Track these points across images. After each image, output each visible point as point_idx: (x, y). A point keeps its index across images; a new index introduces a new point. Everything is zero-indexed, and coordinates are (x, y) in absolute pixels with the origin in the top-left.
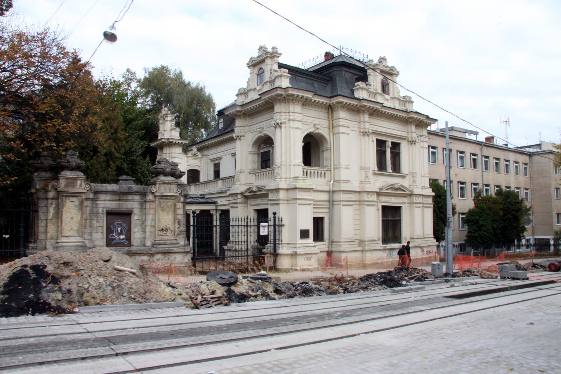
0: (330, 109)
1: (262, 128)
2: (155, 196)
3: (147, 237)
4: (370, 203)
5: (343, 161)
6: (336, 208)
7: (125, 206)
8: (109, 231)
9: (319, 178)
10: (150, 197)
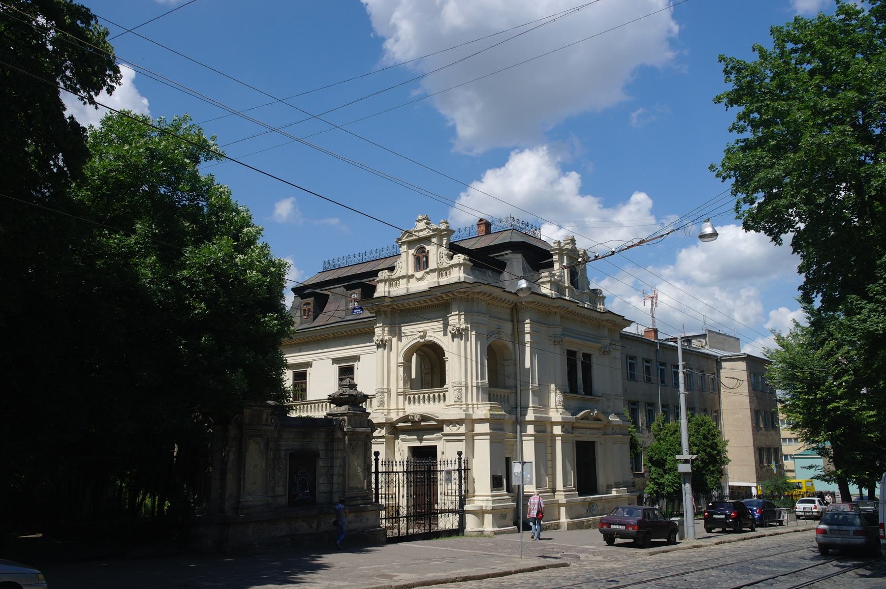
1: (425, 332)
3: (334, 490)
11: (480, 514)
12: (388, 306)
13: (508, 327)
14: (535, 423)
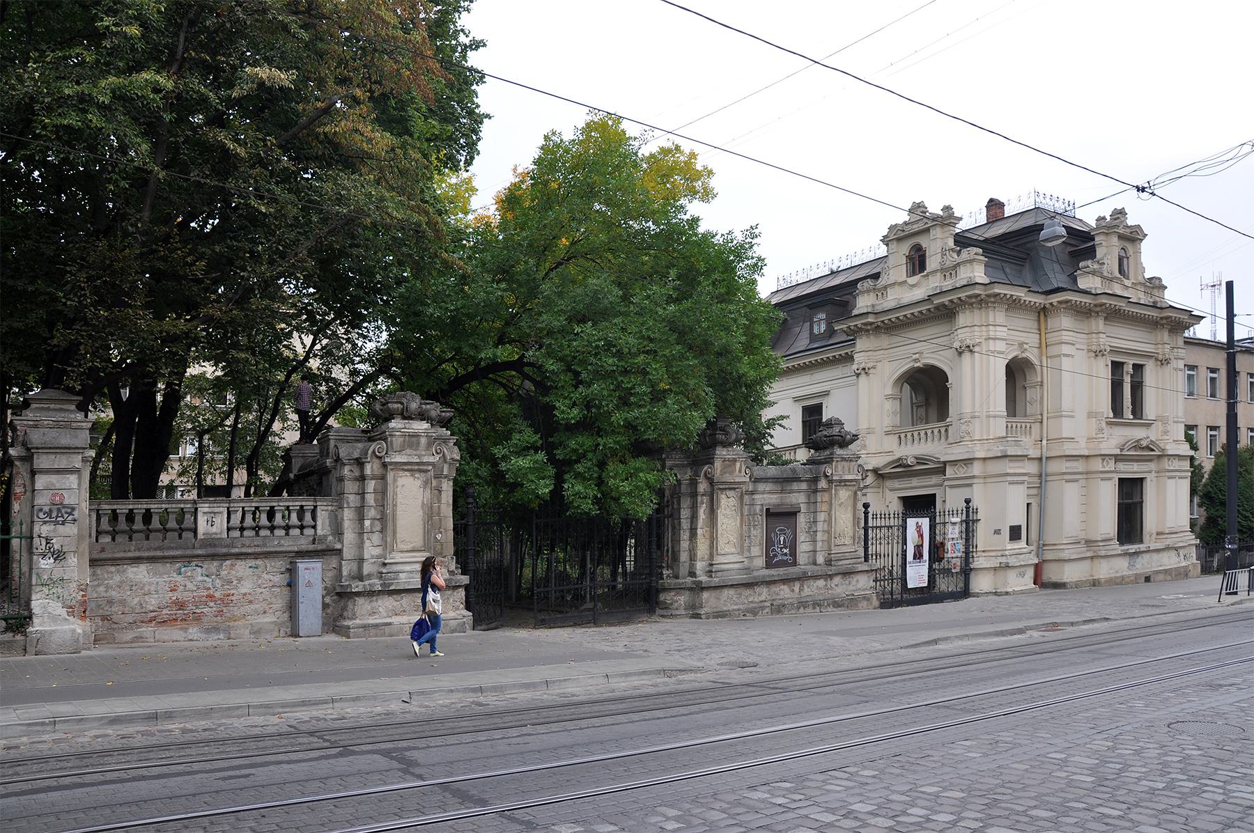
0: (1043, 312)
2: (830, 482)
4: (1104, 475)
5: (1066, 404)
6: (1053, 488)
7: (788, 501)
8: (769, 543)
10: (823, 484)
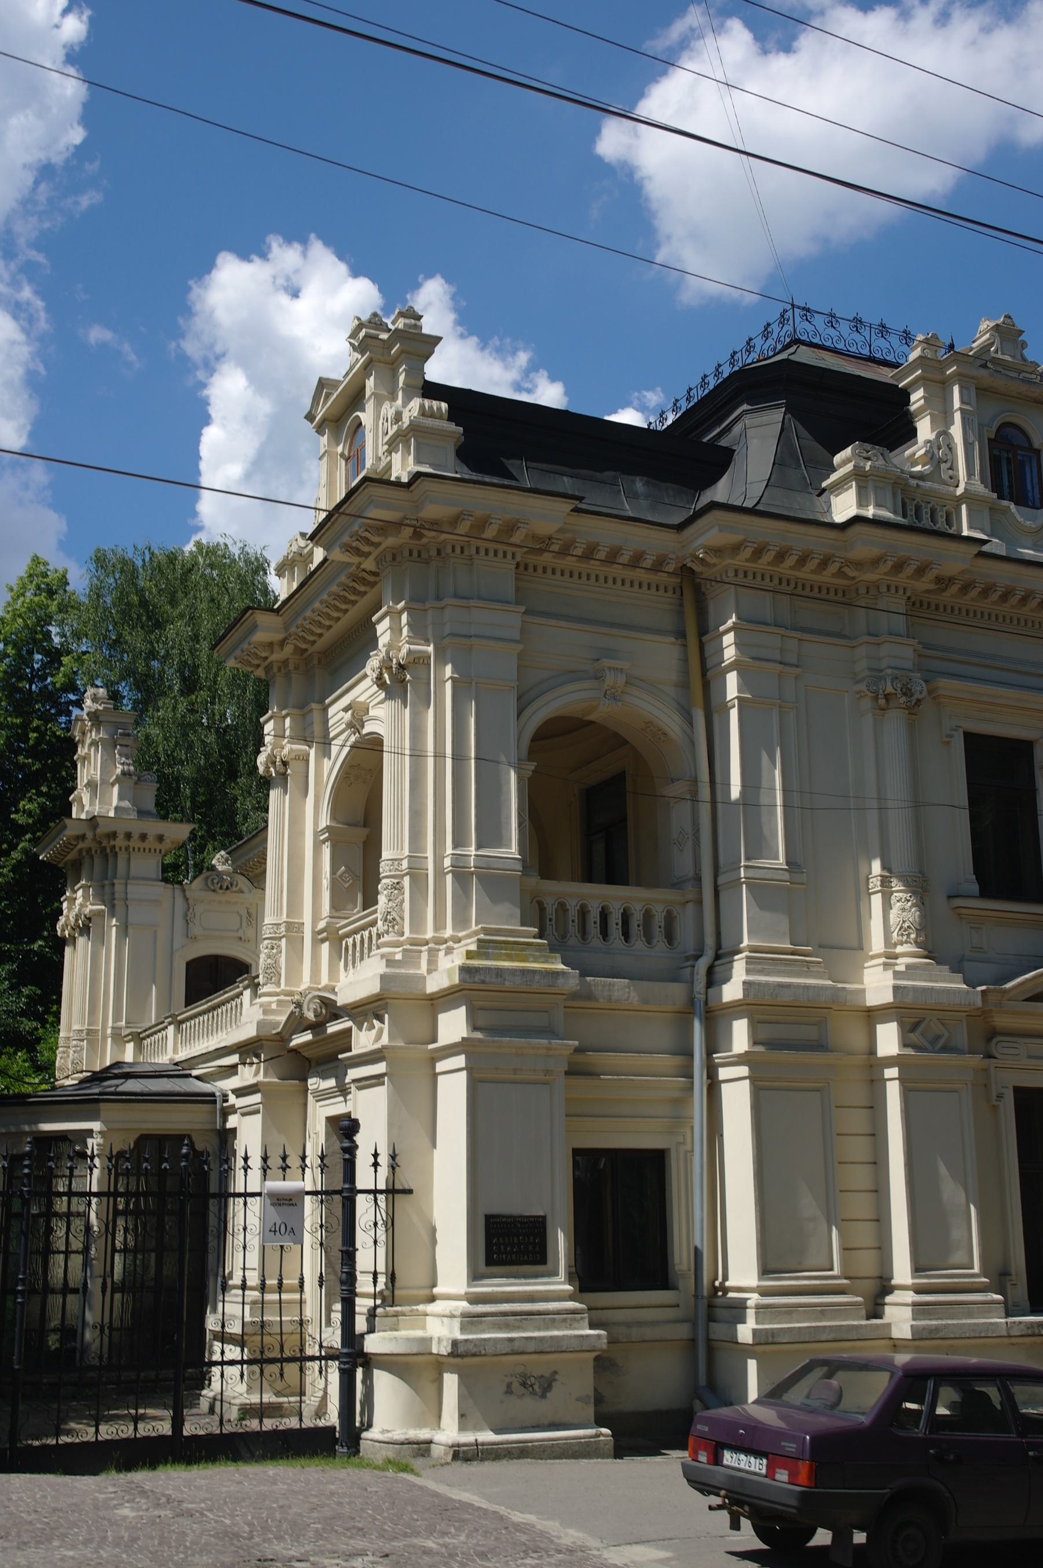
9: (638, 944)
11: (417, 1368)
12: (282, 643)
13: (661, 657)
14: (752, 1006)
